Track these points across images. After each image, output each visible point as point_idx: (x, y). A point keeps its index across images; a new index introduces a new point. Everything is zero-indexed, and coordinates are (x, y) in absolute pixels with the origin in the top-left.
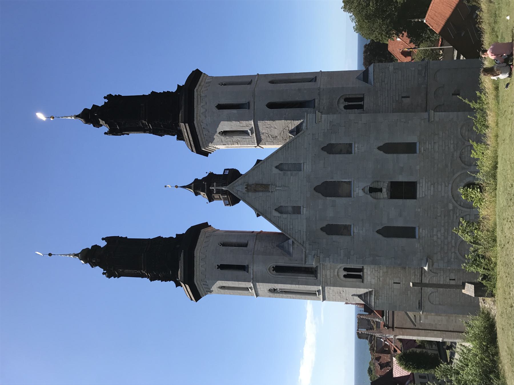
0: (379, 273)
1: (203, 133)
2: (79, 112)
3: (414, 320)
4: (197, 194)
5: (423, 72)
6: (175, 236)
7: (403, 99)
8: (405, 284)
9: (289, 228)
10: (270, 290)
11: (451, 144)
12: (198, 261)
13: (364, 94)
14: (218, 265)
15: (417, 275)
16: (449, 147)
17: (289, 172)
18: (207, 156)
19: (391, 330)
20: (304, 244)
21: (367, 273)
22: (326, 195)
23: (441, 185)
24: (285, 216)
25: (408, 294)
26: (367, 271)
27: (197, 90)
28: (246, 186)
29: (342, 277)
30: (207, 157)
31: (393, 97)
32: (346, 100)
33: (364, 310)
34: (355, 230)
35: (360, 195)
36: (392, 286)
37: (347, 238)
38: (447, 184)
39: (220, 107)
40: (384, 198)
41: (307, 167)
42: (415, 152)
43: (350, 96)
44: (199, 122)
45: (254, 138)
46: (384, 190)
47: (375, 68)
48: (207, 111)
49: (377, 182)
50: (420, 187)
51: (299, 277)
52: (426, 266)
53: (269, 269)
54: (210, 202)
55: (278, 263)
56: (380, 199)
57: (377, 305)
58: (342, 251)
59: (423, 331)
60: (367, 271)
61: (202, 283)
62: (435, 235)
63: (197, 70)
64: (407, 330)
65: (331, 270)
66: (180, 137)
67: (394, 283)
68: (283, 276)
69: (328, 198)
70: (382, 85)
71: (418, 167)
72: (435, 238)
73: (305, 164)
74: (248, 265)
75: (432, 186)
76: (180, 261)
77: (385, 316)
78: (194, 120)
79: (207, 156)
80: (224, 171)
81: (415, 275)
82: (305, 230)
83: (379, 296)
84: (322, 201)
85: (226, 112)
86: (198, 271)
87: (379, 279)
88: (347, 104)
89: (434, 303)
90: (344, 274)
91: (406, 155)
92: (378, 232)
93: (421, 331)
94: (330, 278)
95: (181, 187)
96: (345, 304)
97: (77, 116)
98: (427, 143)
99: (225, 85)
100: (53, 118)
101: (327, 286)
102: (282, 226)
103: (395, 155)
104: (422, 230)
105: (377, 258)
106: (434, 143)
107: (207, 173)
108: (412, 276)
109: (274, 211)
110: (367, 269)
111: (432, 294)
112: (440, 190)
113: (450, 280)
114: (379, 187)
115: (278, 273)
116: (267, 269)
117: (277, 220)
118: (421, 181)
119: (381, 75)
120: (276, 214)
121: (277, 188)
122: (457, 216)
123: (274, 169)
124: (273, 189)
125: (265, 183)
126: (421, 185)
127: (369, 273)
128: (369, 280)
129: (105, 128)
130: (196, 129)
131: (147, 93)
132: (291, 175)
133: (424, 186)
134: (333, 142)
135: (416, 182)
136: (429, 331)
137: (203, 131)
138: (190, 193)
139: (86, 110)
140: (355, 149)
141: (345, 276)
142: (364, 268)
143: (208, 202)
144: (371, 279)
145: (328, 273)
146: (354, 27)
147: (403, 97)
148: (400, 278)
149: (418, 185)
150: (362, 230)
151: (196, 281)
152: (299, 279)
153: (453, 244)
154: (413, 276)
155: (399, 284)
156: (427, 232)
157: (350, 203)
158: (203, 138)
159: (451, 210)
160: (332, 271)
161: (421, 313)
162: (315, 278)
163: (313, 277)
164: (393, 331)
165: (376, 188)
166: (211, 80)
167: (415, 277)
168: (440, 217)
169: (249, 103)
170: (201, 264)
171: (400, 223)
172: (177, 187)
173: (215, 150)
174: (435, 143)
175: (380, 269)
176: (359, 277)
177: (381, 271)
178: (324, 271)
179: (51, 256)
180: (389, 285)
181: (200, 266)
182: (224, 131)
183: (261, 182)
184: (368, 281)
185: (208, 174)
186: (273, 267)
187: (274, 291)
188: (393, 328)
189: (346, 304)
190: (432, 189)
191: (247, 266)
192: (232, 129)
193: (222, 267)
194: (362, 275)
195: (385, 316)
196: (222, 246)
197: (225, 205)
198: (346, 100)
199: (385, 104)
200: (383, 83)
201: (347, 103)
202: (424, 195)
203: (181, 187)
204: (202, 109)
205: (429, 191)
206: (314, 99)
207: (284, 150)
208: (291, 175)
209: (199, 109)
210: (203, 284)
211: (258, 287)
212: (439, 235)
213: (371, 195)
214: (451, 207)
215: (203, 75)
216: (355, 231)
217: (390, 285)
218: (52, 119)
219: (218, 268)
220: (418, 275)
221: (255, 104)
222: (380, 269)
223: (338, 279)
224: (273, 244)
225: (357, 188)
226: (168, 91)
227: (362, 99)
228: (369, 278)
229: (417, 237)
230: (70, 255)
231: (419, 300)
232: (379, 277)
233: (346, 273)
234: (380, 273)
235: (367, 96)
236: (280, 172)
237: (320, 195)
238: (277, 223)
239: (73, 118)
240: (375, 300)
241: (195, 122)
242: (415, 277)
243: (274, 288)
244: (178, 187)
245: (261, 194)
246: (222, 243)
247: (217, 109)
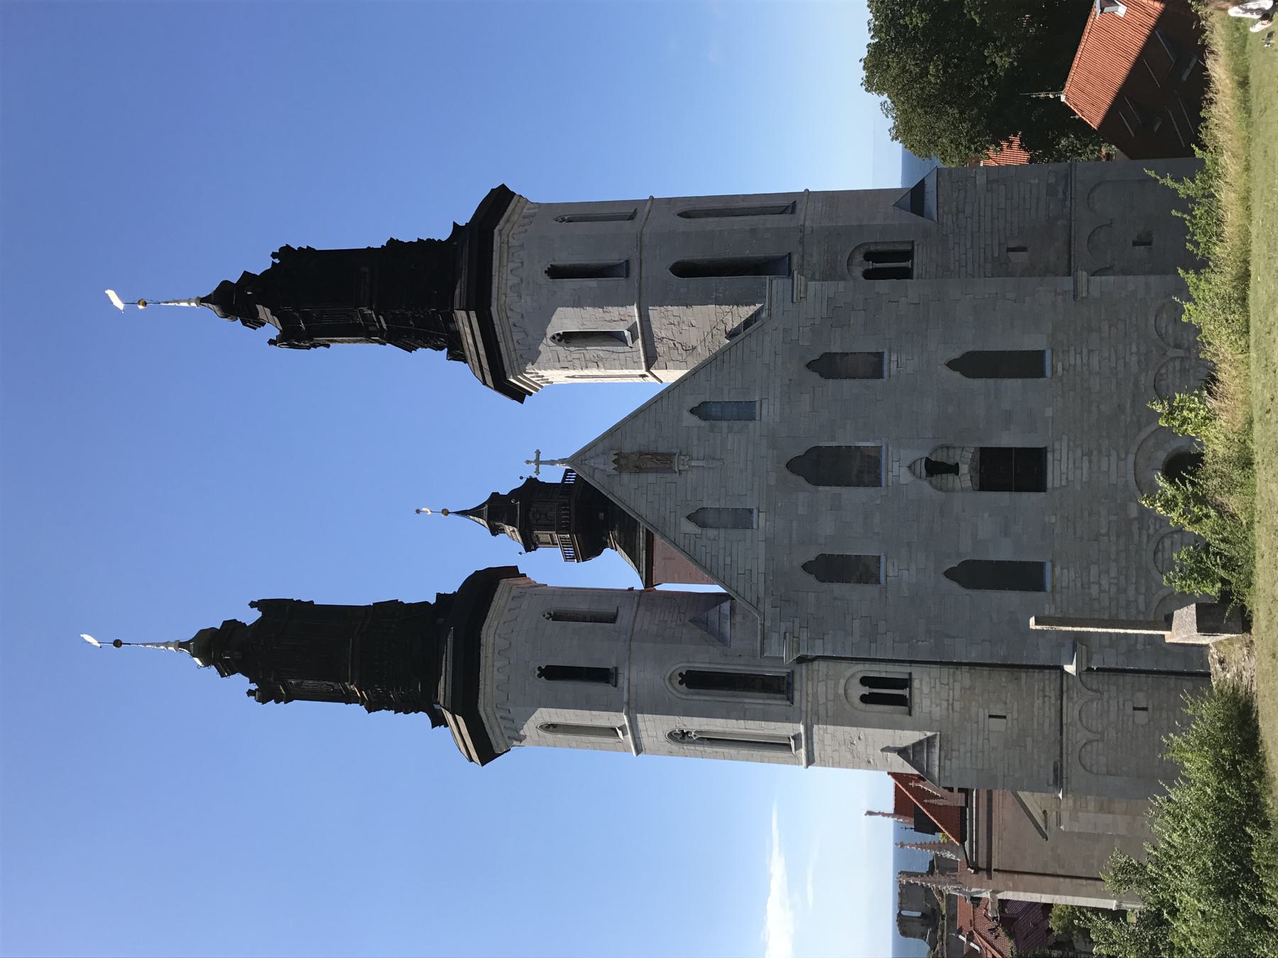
0: (951, 691)
1: (512, 338)
2: (209, 288)
3: (1042, 825)
4: (495, 531)
5: (1060, 189)
6: (433, 601)
7: (1011, 254)
8: (1017, 719)
9: (721, 563)
10: (672, 736)
11: (1131, 354)
12: (490, 655)
13: (913, 242)
14: (540, 668)
15: (1050, 698)
16: (1127, 360)
17: (724, 424)
18: (521, 401)
19: (984, 875)
20: (759, 605)
21: (921, 689)
22: (817, 480)
23: (1109, 456)
24: (712, 533)
25: (1025, 747)
26: (921, 684)
27: (500, 231)
28: (616, 457)
29: (857, 701)
30: (522, 403)
31: (985, 249)
32: (869, 256)
33: (913, 827)
34: (889, 570)
35: (901, 482)
36: (986, 723)
37: (870, 590)
38: (1123, 456)
39: (556, 273)
41: (769, 412)
42: (1040, 373)
43: (879, 248)
44: (503, 308)
45: (639, 350)
46: (964, 469)
47: (940, 179)
48: (524, 282)
49: (945, 450)
50: (1056, 462)
51: (746, 701)
52: (1071, 664)
53: (670, 679)
54: (527, 551)
55: (694, 662)
56: (953, 490)
57: (947, 774)
58: (856, 623)
59: (1068, 880)
60: (921, 684)
61: (498, 716)
62: (1094, 583)
63: (503, 188)
64: (1026, 877)
65: (829, 682)
66: (457, 354)
67: (990, 716)
68: (705, 698)
69: (820, 488)
70: (957, 218)
71: (1049, 412)
72: (1094, 590)
73: (765, 402)
74: (616, 669)
75: (1085, 458)
76: (444, 656)
77: (968, 841)
78: (490, 305)
79: (521, 401)
80: (565, 477)
81: (1044, 696)
82: (762, 569)
83: (952, 750)
84: (806, 496)
85: (570, 284)
86: (488, 682)
87: (952, 704)
88: (871, 267)
89: (1094, 769)
90: (864, 693)
91: (1018, 383)
92: (950, 574)
93: (1062, 880)
94: (825, 704)
95: (457, 513)
96: (866, 815)
97: (203, 301)
98: (1072, 352)
99: (569, 221)
100: (145, 304)
101: (818, 724)
102: (703, 558)
103: (991, 381)
104: (1062, 568)
105: (947, 641)
106: (1090, 351)
107: (521, 478)
108: (1036, 699)
109: (684, 521)
110: (921, 681)
111: (1089, 747)
112: (1104, 468)
113: (1135, 709)
114: (951, 462)
115: (691, 690)
116: (664, 679)
117: (692, 542)
118: (1057, 445)
119: (955, 195)
120: (690, 528)
121: (693, 463)
122: (1149, 536)
123: (686, 414)
124: (683, 465)
125: (662, 449)
126: (1057, 456)
127: (926, 690)
128: (926, 710)
129: (272, 329)
130: (496, 326)
131: (378, 242)
132: (730, 430)
133: (1064, 459)
134: (835, 348)
135: (1045, 448)
136: (1084, 882)
137: (511, 332)
139: (225, 284)
140: (891, 365)
141: (864, 699)
142: (914, 676)
143: (523, 551)
144: (931, 707)
145: (821, 689)
146: (889, 130)
147: (1010, 250)
148: (1005, 703)
149: (1050, 456)
150: (908, 570)
151: (484, 707)
152: (746, 706)
153: (1142, 607)
154: (1038, 699)
155: (1004, 720)
156: (1072, 573)
157: (878, 502)
158: (512, 349)
159: (1135, 519)
160: (831, 683)
161: (1060, 795)
162: (788, 703)
163: (781, 699)
164: (988, 879)
165: (942, 463)
166: (536, 211)
167: (1044, 702)
168: (1106, 538)
169: (627, 262)
170: (498, 664)
171: (1004, 553)
172: (446, 512)
173: (542, 387)
174: (1092, 351)
175: (954, 681)
176: (902, 701)
177: (958, 686)
178: (810, 684)
179: (121, 648)
180: (977, 722)
181: (495, 669)
182: (564, 332)
183: (652, 449)
184: (924, 711)
185: (524, 481)
186: (681, 675)
187: (681, 738)
188: (988, 870)
189: (868, 816)
190: (1086, 465)
191: (614, 670)
192: (584, 327)
193: (551, 673)
194: (908, 697)
195: (968, 841)
196: (553, 620)
197: (566, 560)
198: (869, 256)
199: (966, 266)
200: (961, 215)
201: (871, 265)
202: (1064, 483)
203: (457, 513)
204: (510, 277)
205: (1078, 472)
206: (790, 254)
207: (713, 369)
208: (730, 430)
209: (504, 276)
210: (501, 717)
211: (641, 725)
212: (1104, 582)
213: (931, 482)
215: (515, 198)
216: (891, 573)
217: (981, 719)
218: (141, 307)
219: (540, 676)
220: (1052, 694)
221: (643, 265)
222: (954, 681)
223: (847, 707)
224: (683, 615)
225: (896, 465)
226: (428, 240)
227: (908, 255)
228: (926, 702)
229: (1049, 587)
230: (167, 644)
231: (1055, 763)
232: (951, 702)
233: (866, 690)
234: (953, 690)
235: (920, 247)
236: (703, 423)
237: (801, 480)
238: (692, 549)
239: (193, 304)
240: (942, 761)
241: (494, 309)
242: (1044, 702)
243: (682, 728)
244: (449, 513)
245: (652, 477)
246: (552, 613)
247: (548, 278)
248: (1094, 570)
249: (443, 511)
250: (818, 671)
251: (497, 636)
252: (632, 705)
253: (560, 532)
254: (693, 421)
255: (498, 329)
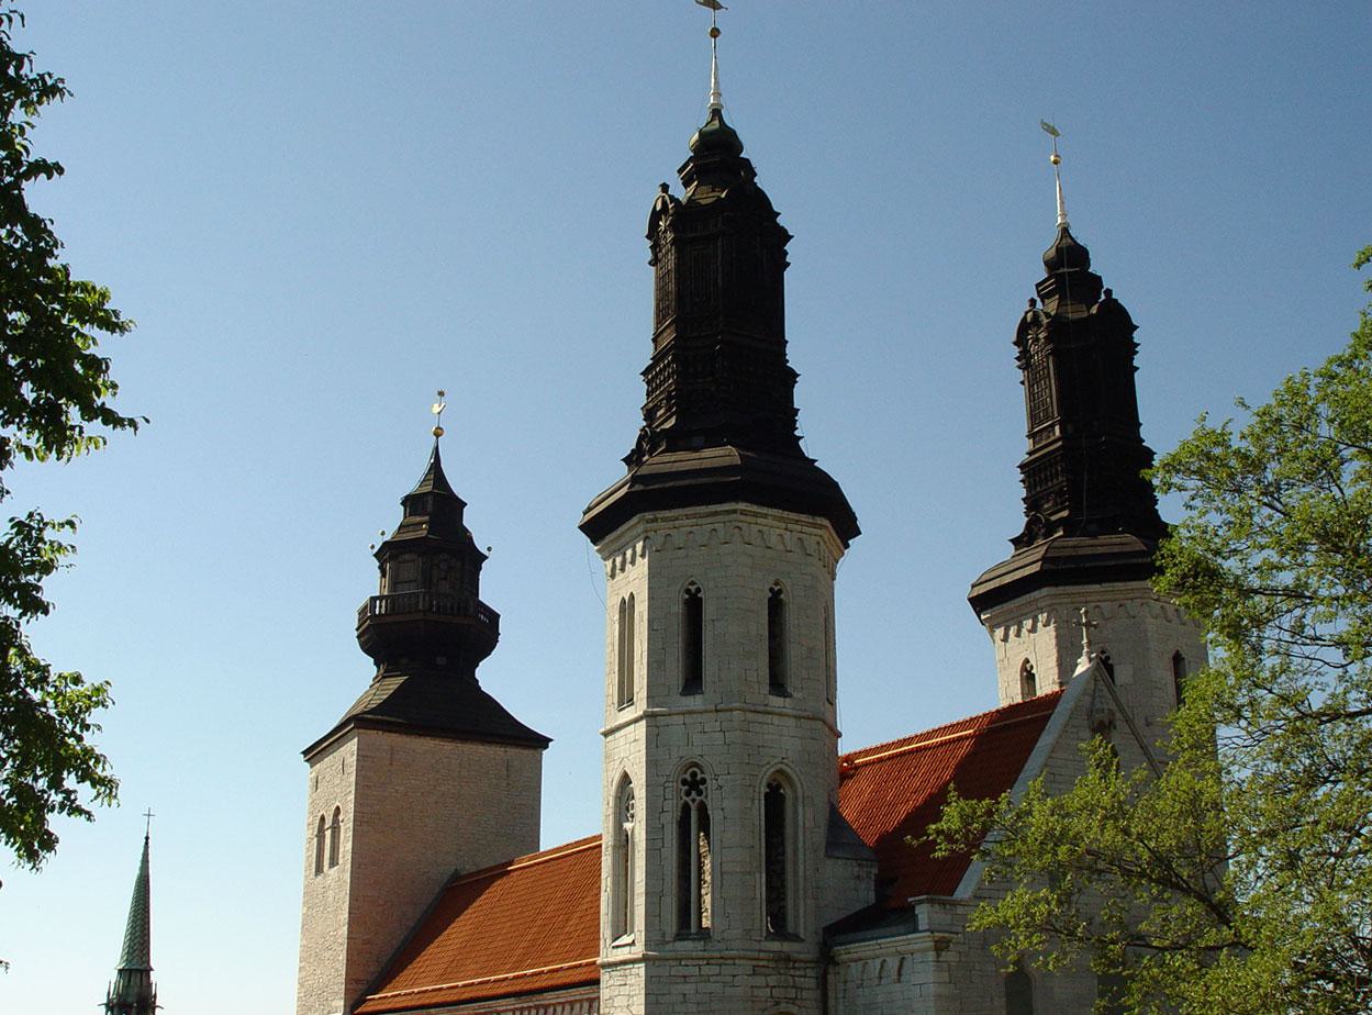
1: (1104, 601)
14: (780, 591)
97: (1065, 231)
100: (1056, 162)
138: (412, 479)
152: (757, 875)
172: (438, 434)
186: (779, 786)
203: (437, 449)
218: (1052, 158)
230: (717, 94)
249: (441, 429)
250: (805, 976)
251: (818, 538)
252: (750, 716)
253: (427, 598)
255: (1119, 585)
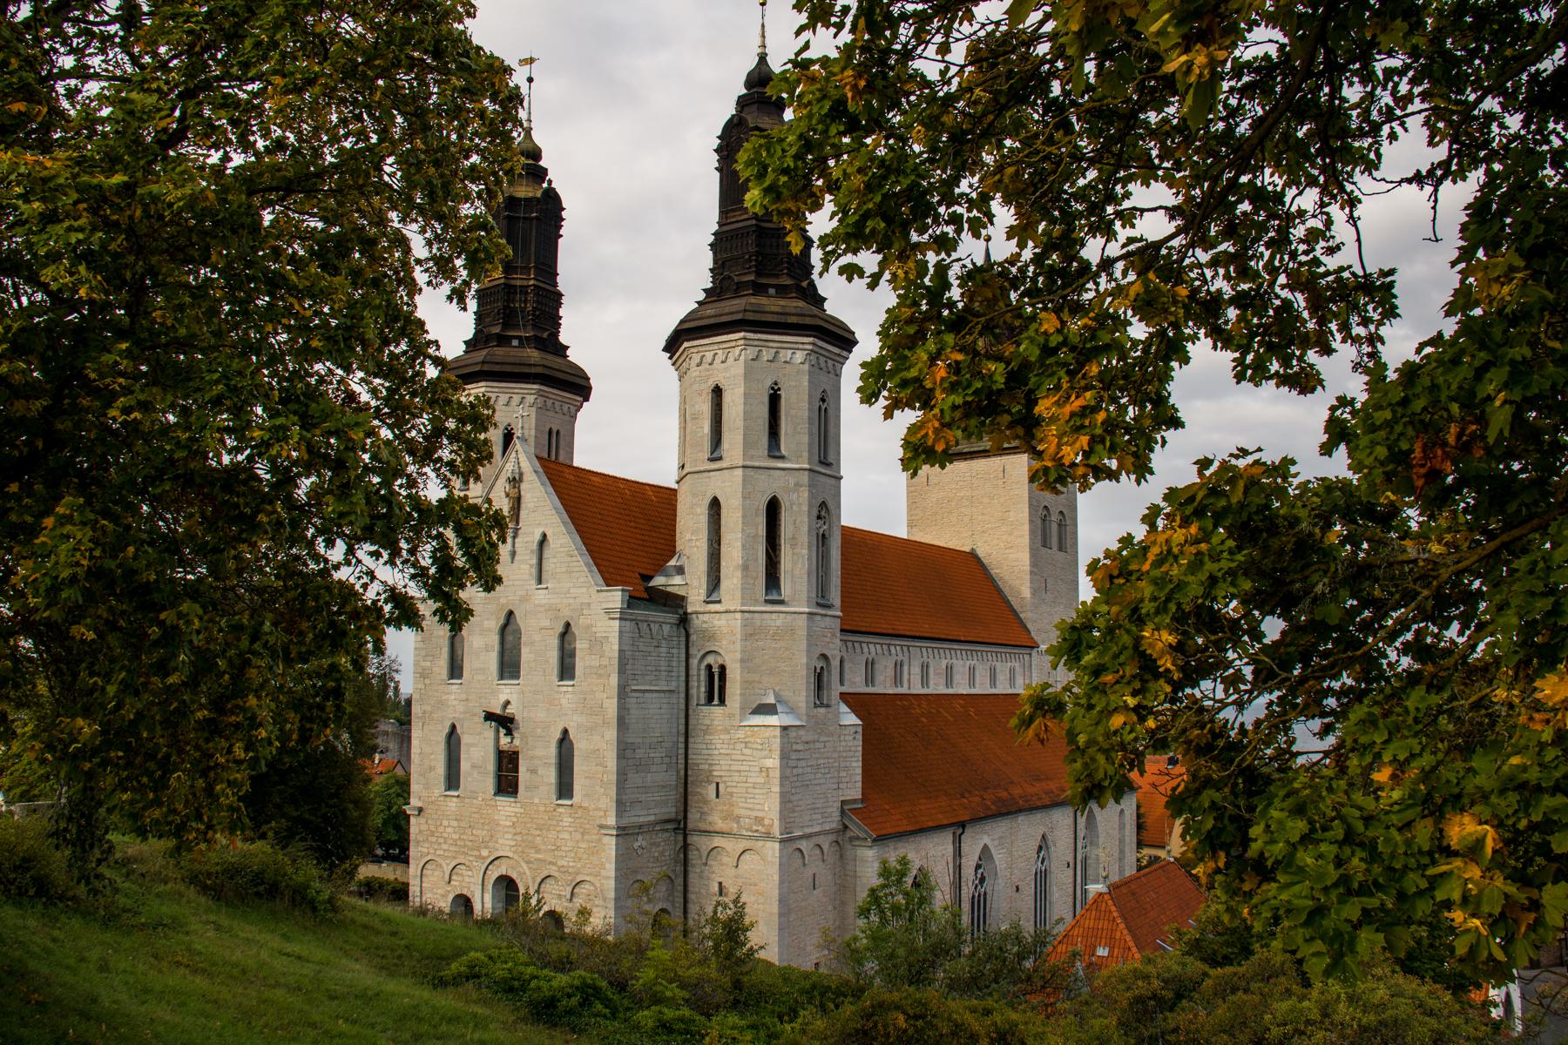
32: (723, 668)
34: (455, 687)
40: (497, 739)
42: (560, 797)
71: (536, 801)
72: (445, 823)
84: (494, 624)
85: (705, 407)
125: (523, 514)
201: (716, 670)
214: (485, 853)
248: (455, 824)
254: (538, 537)
